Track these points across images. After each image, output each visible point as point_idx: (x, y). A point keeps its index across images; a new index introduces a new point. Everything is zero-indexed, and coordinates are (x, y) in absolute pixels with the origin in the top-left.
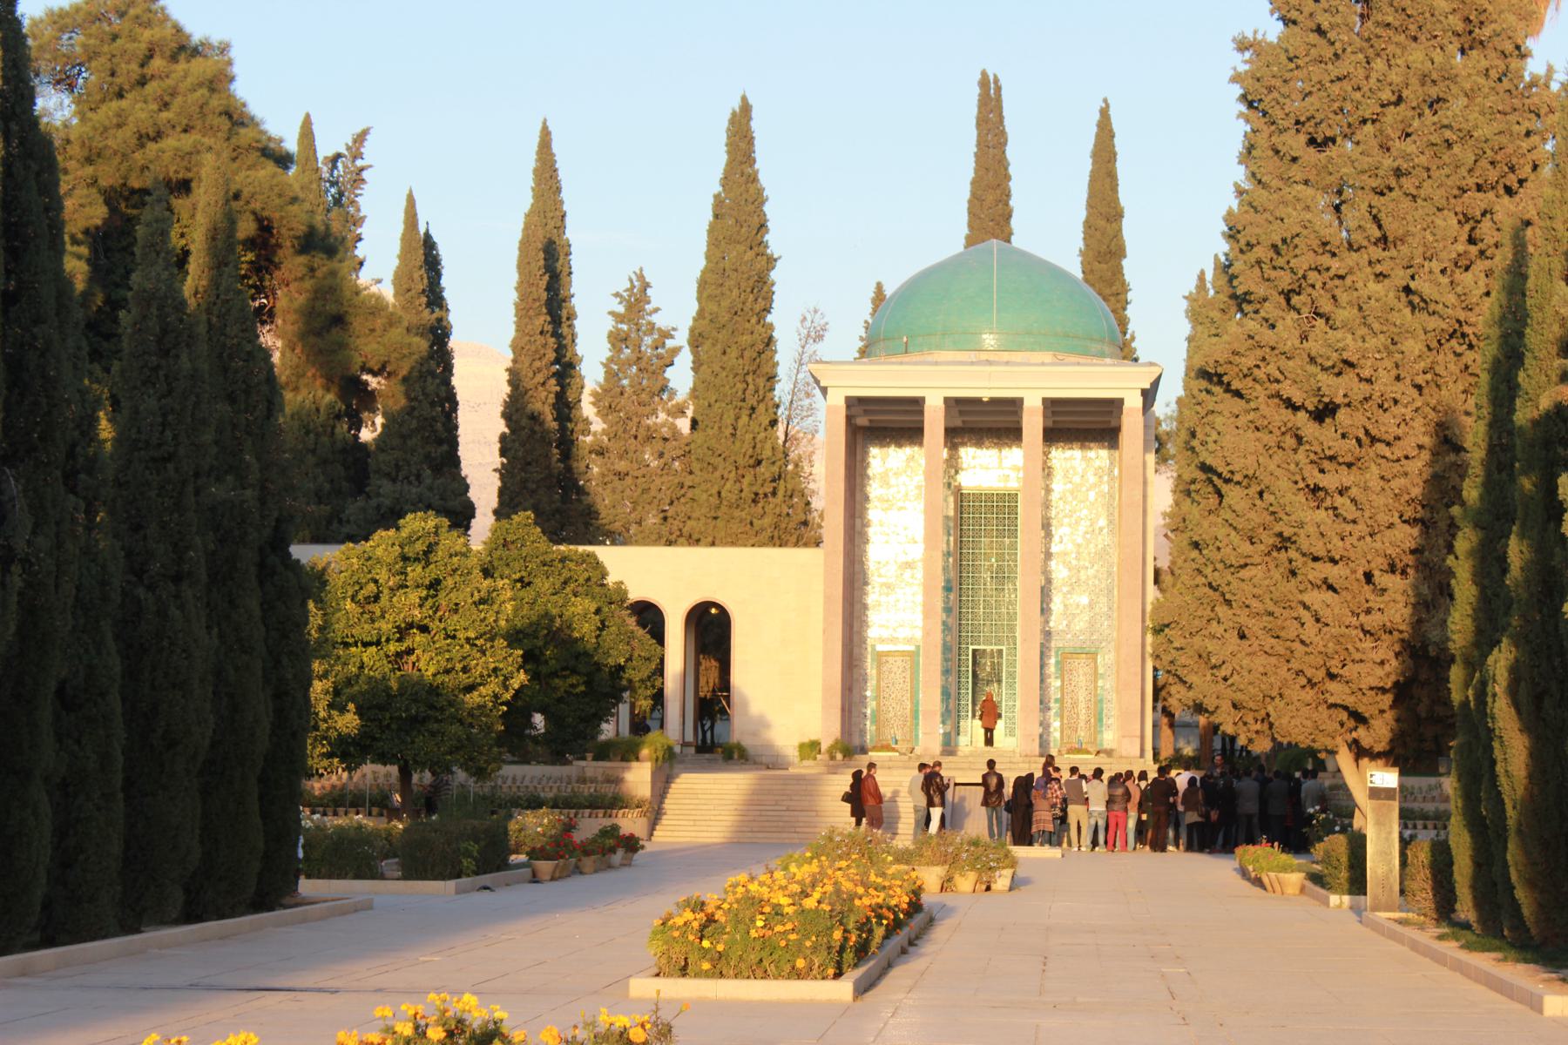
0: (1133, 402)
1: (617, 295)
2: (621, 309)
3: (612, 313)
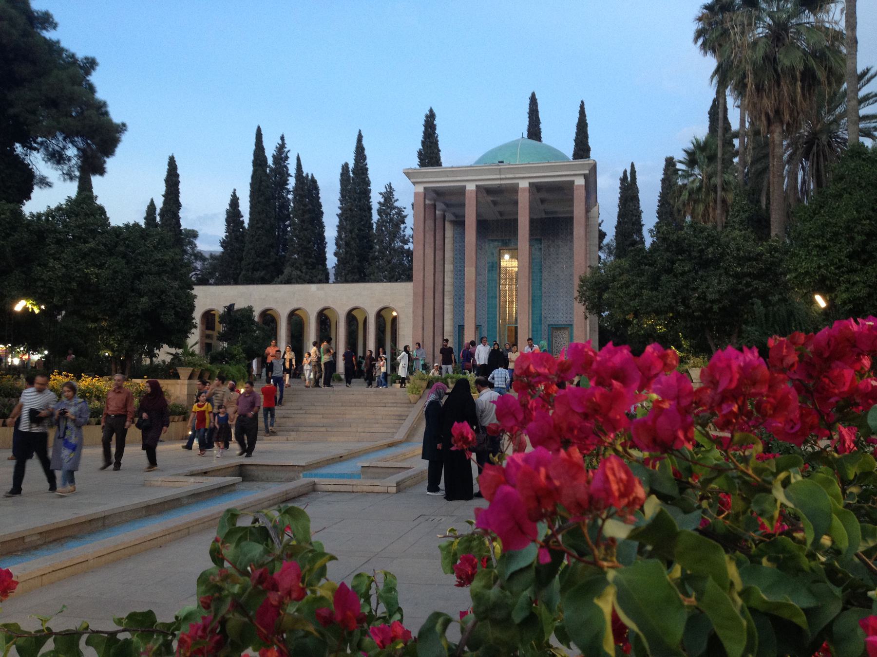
0: (580, 182)
1: (381, 194)
2: (382, 200)
3: (380, 203)
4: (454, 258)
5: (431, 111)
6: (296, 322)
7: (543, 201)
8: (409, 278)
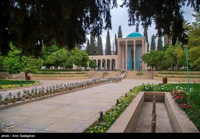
4: (124, 51)
5: (120, 26)
6: (99, 61)
7: (138, 42)
8: (117, 54)
